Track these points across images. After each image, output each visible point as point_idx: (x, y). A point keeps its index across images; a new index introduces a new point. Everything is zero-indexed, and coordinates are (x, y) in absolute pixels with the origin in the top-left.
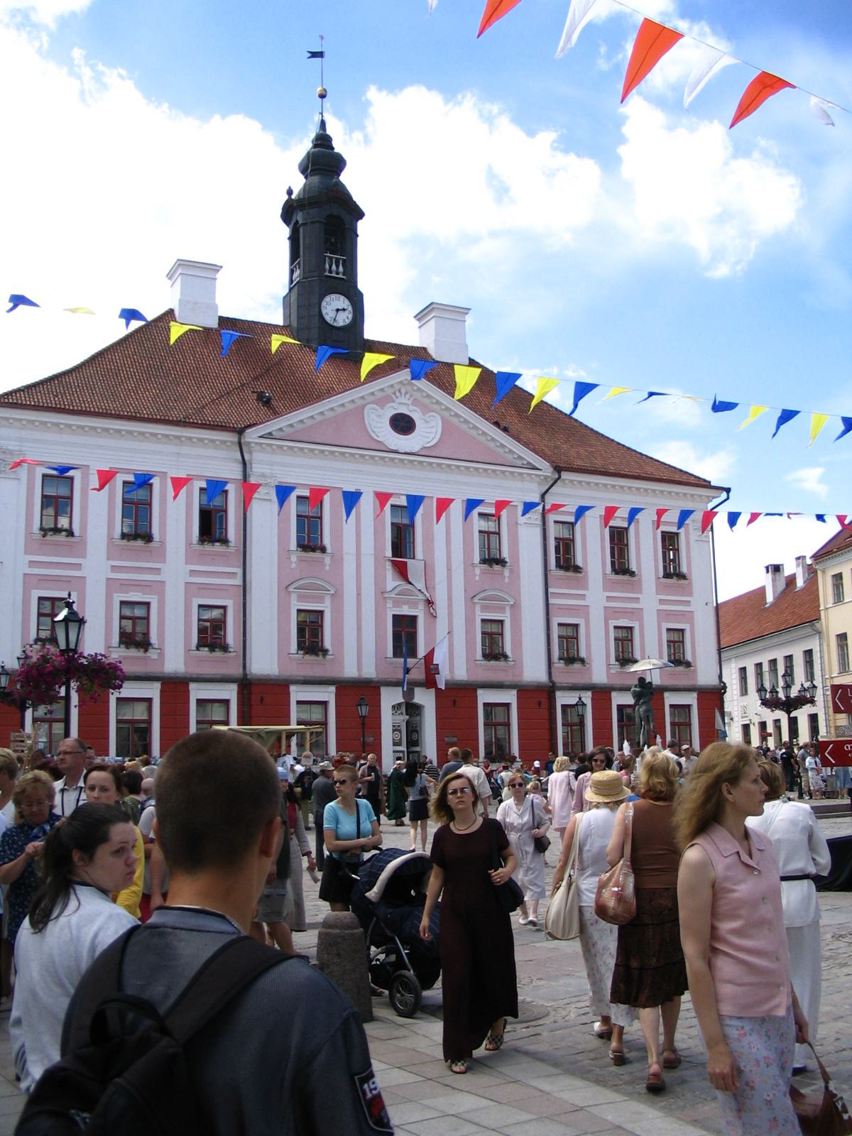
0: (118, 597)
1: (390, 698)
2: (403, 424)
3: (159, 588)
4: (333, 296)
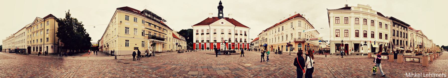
1: (221, 44)
2: (222, 23)
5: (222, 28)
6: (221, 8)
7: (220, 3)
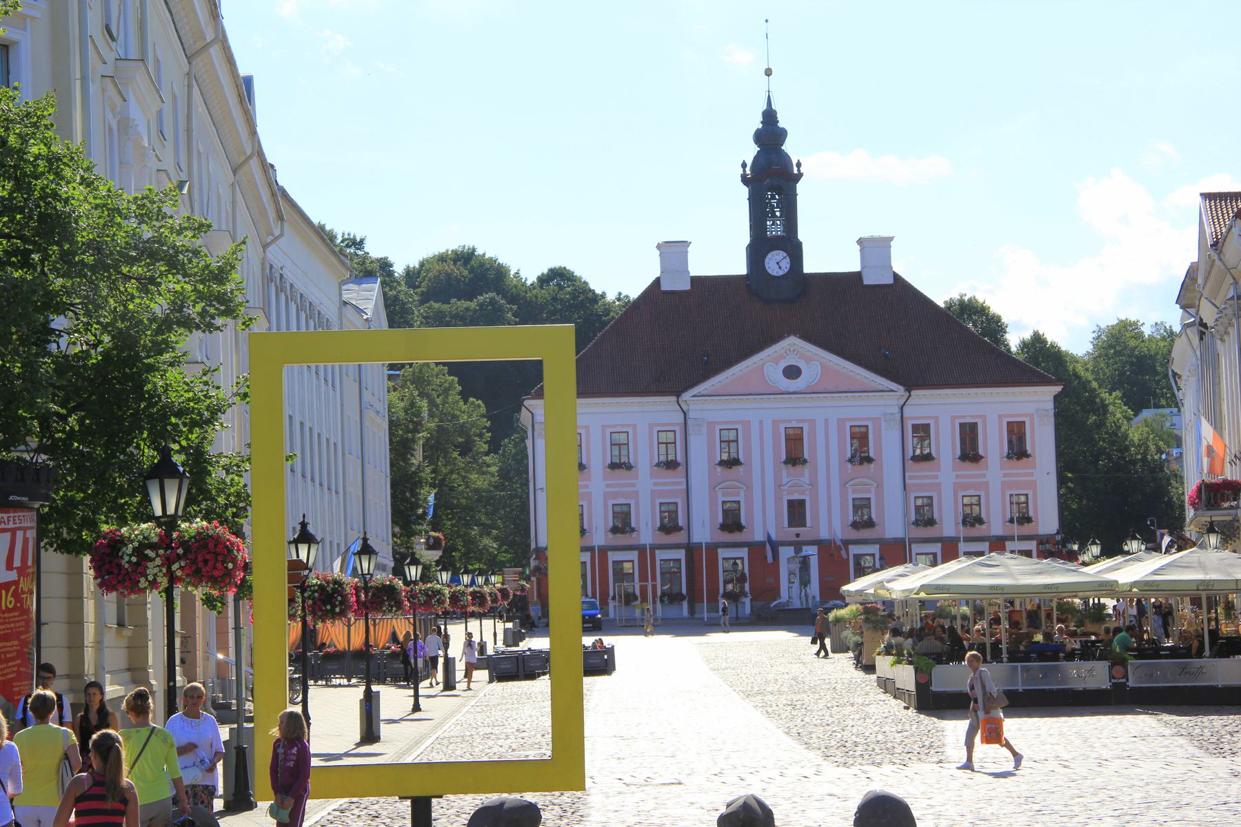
0: (611, 502)
1: (786, 553)
2: (792, 372)
3: (636, 494)
4: (774, 253)
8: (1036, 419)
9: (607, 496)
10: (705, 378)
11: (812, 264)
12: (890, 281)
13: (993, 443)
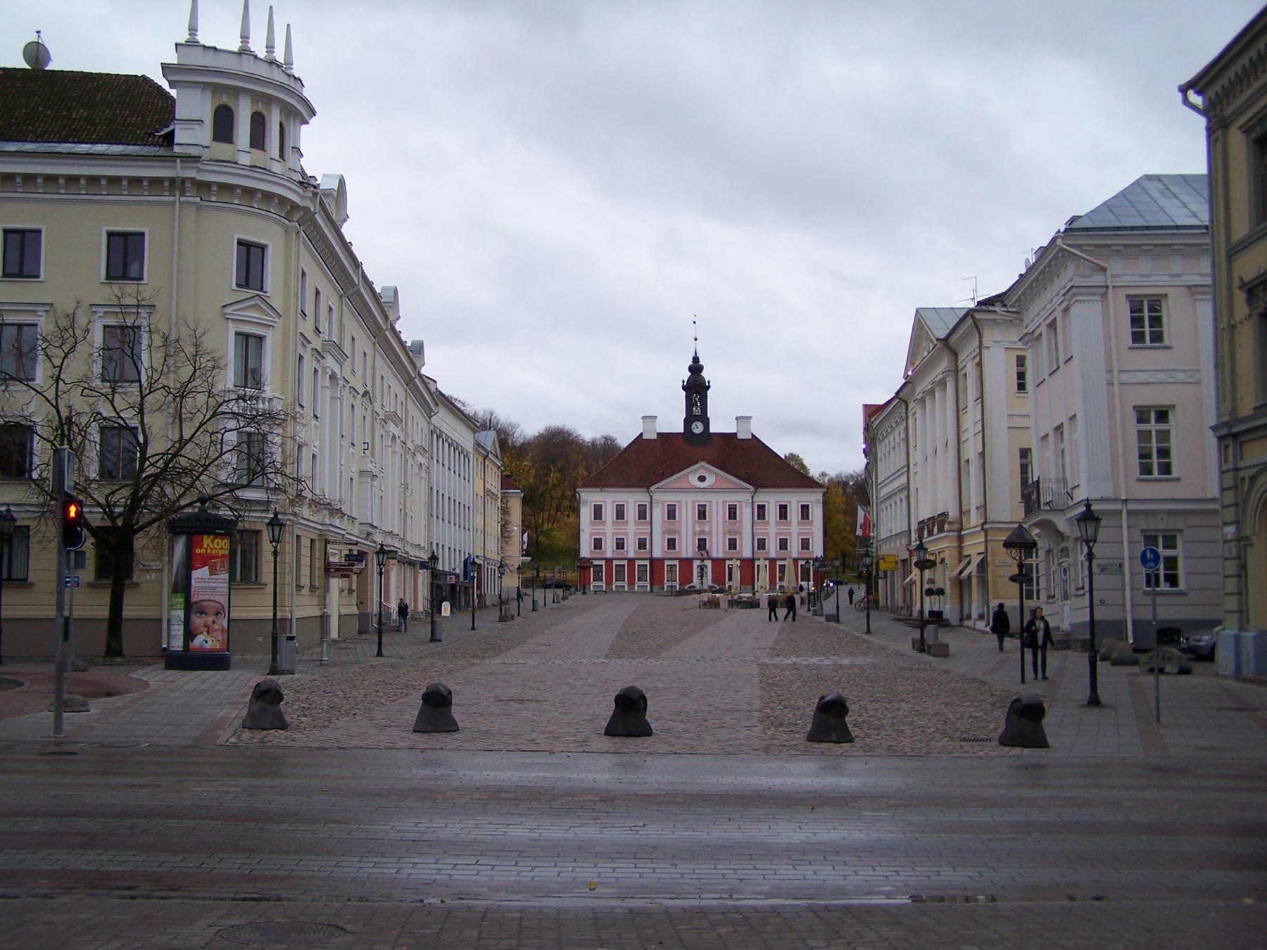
1: (696, 563)
2: (702, 479)
3: (627, 534)
5: (702, 499)
6: (696, 388)
7: (696, 368)
8: (815, 505)
9: (614, 534)
10: (662, 479)
11: (712, 430)
12: (750, 437)
13: (794, 513)
